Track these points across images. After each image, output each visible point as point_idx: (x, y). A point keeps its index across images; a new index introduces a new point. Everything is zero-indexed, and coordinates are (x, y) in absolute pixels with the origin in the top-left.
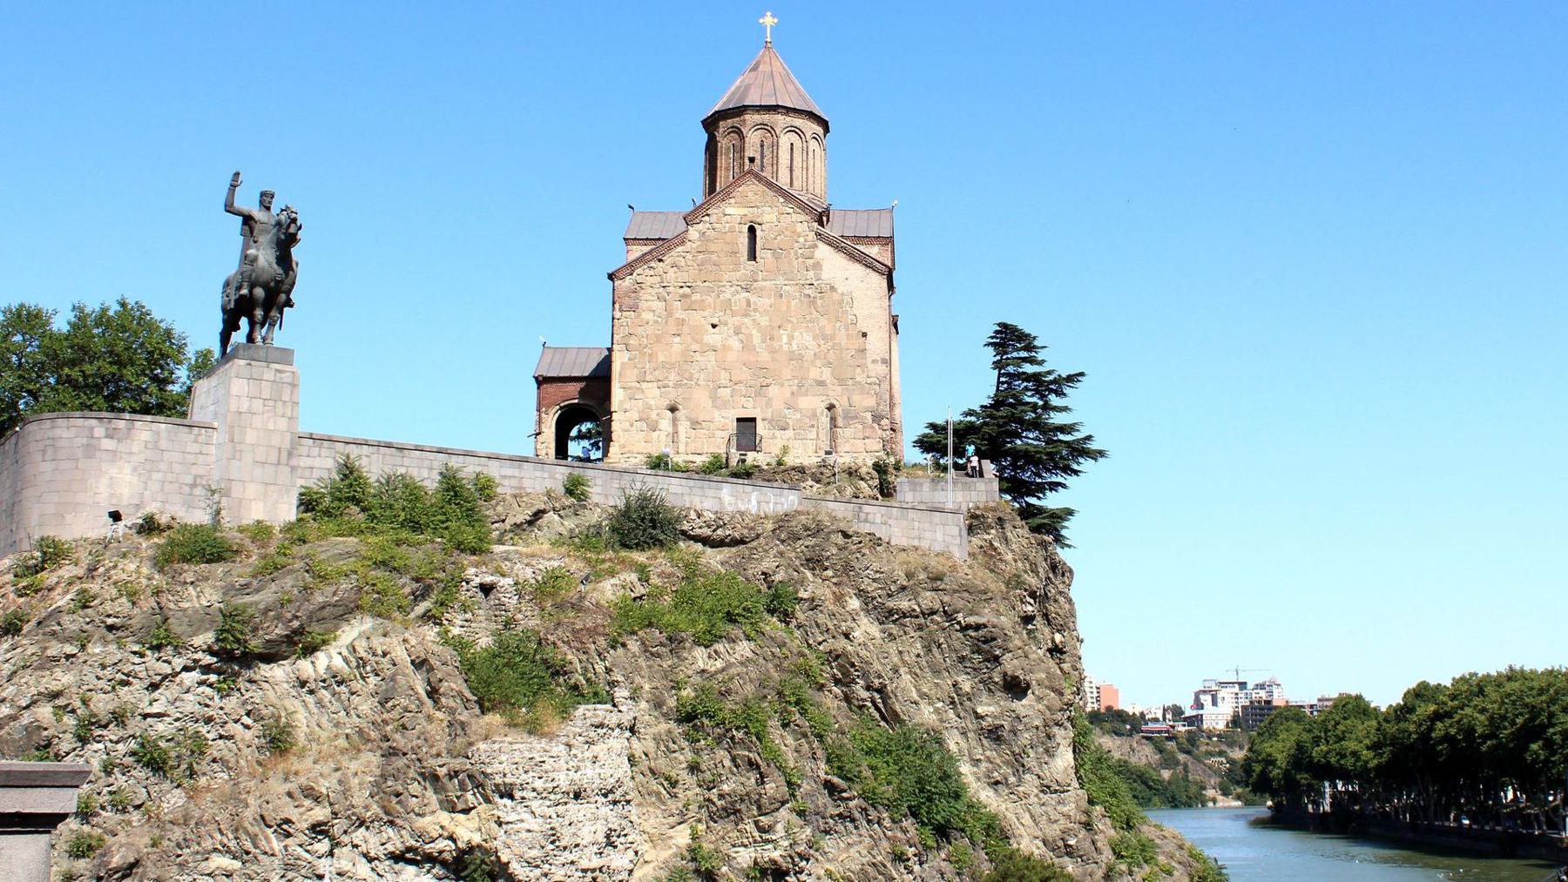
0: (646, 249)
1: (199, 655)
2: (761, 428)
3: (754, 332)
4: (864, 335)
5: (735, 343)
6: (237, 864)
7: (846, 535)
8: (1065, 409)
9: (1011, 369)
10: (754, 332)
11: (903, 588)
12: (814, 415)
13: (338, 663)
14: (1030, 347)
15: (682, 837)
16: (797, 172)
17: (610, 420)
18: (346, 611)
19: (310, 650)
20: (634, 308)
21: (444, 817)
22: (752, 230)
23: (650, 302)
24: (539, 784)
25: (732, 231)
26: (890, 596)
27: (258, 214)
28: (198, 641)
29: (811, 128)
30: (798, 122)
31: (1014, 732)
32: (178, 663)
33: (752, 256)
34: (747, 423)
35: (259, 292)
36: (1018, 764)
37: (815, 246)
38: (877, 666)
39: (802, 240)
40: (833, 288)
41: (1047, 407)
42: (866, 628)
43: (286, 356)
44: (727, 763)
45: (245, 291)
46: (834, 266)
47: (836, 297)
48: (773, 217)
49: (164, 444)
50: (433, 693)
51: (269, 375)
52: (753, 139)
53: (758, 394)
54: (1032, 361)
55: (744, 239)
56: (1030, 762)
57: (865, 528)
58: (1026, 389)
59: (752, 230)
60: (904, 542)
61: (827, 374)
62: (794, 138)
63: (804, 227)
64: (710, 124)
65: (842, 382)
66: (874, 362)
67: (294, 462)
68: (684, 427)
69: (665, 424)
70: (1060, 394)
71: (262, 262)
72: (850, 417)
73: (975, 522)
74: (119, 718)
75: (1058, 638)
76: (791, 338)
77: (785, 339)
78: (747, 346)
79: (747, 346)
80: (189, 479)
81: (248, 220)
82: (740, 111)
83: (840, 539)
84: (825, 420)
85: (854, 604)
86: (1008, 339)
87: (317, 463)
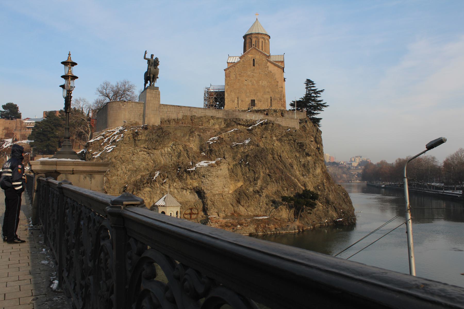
0: (232, 64)
1: (142, 149)
2: (256, 102)
5: (250, 83)
6: (151, 190)
7: (273, 124)
9: (309, 89)
12: (267, 99)
13: (169, 150)
14: (313, 84)
16: (263, 47)
17: (224, 101)
20: (229, 77)
21: (191, 181)
23: (233, 76)
24: (209, 174)
25: (249, 60)
27: (151, 60)
28: (142, 146)
30: (263, 36)
31: (308, 165)
32: (138, 150)
34: (253, 102)
35: (152, 76)
36: (308, 171)
38: (279, 151)
42: (277, 144)
43: (157, 88)
44: (248, 170)
45: (148, 75)
46: (271, 68)
47: (272, 74)
48: (257, 57)
49: (134, 107)
51: (154, 92)
52: (254, 40)
53: (255, 94)
56: (311, 170)
57: (277, 123)
58: (313, 93)
59: (254, 60)
60: (285, 125)
61: (270, 91)
62: (263, 40)
63: (264, 59)
64: (245, 37)
65: (273, 92)
67: (160, 110)
68: (240, 102)
69: (236, 101)
71: (152, 69)
72: (274, 99)
73: (301, 121)
75: (318, 146)
76: (262, 83)
78: (253, 84)
79: (253, 84)
80: (139, 114)
81: (149, 61)
82: (251, 34)
83: (271, 125)
84: (269, 100)
85: (274, 138)
86: (309, 82)
87: (164, 110)
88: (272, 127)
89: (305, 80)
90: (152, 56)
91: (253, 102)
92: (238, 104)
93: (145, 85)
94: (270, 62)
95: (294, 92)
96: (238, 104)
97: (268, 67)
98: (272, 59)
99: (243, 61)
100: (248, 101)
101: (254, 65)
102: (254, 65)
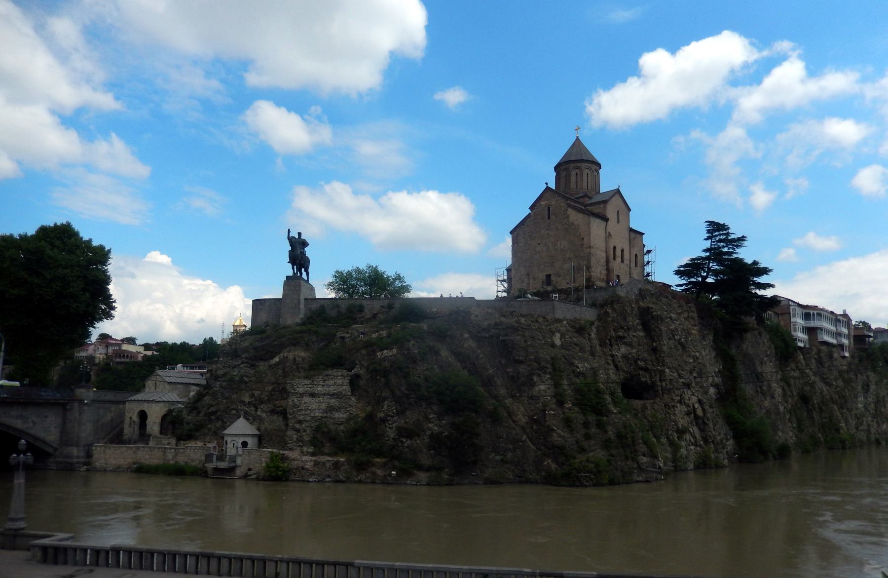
2: (553, 278)
11: (484, 329)
15: (369, 409)
18: (281, 347)
19: (272, 358)
20: (517, 243)
29: (584, 165)
30: (579, 164)
32: (240, 362)
34: (549, 276)
42: (472, 344)
46: (575, 217)
50: (298, 368)
52: (563, 174)
55: (546, 213)
68: (531, 281)
74: (224, 375)
85: (466, 335)
90: (300, 234)
91: (548, 276)
92: (528, 284)
94: (575, 208)
96: (528, 284)
100: (542, 276)
101: (549, 218)
102: (549, 218)
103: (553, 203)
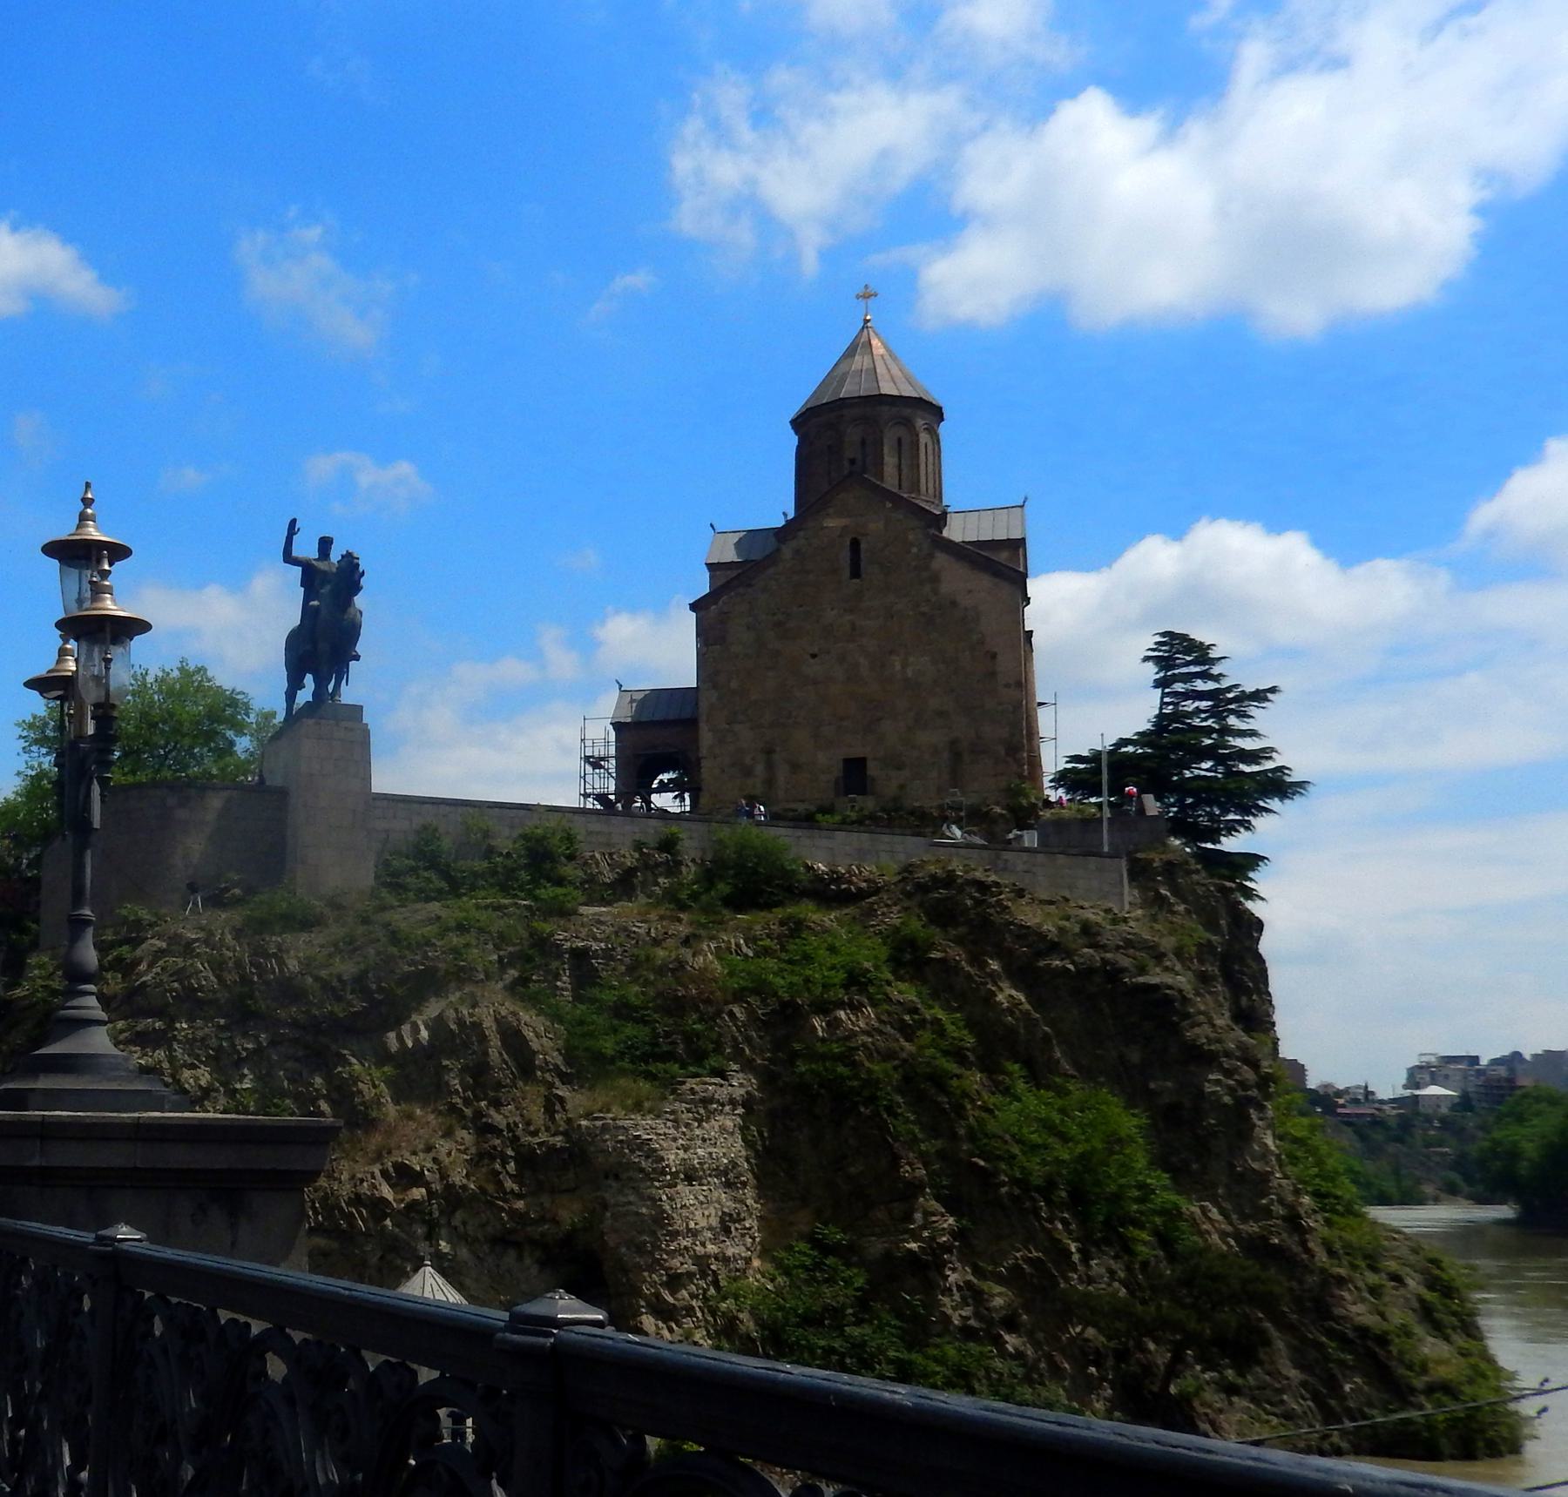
3: (862, 660)
4: (994, 656)
8: (1253, 733)
9: (1179, 687)
10: (862, 660)
22: (855, 544)
26: (1040, 955)
33: (856, 573)
37: (931, 556)
39: (915, 550)
40: (954, 604)
41: (1226, 731)
54: (1205, 676)
55: (845, 555)
66: (1007, 686)
70: (1242, 715)
76: (904, 666)
77: (898, 667)
85: (994, 965)
88: (978, 903)
89: (1147, 641)
93: (290, 697)
95: (1090, 703)
97: (935, 579)
98: (956, 531)
99: (797, 552)
103: (875, 526)
